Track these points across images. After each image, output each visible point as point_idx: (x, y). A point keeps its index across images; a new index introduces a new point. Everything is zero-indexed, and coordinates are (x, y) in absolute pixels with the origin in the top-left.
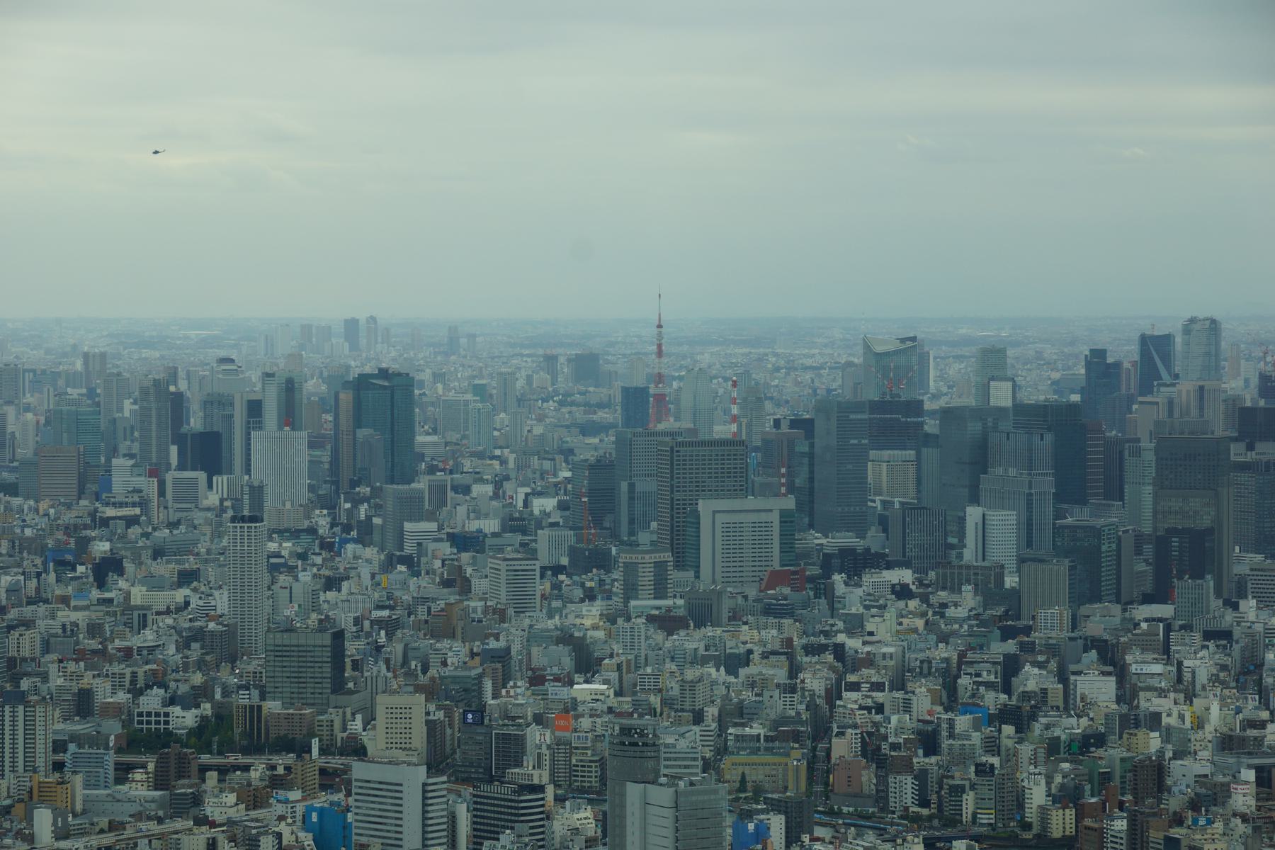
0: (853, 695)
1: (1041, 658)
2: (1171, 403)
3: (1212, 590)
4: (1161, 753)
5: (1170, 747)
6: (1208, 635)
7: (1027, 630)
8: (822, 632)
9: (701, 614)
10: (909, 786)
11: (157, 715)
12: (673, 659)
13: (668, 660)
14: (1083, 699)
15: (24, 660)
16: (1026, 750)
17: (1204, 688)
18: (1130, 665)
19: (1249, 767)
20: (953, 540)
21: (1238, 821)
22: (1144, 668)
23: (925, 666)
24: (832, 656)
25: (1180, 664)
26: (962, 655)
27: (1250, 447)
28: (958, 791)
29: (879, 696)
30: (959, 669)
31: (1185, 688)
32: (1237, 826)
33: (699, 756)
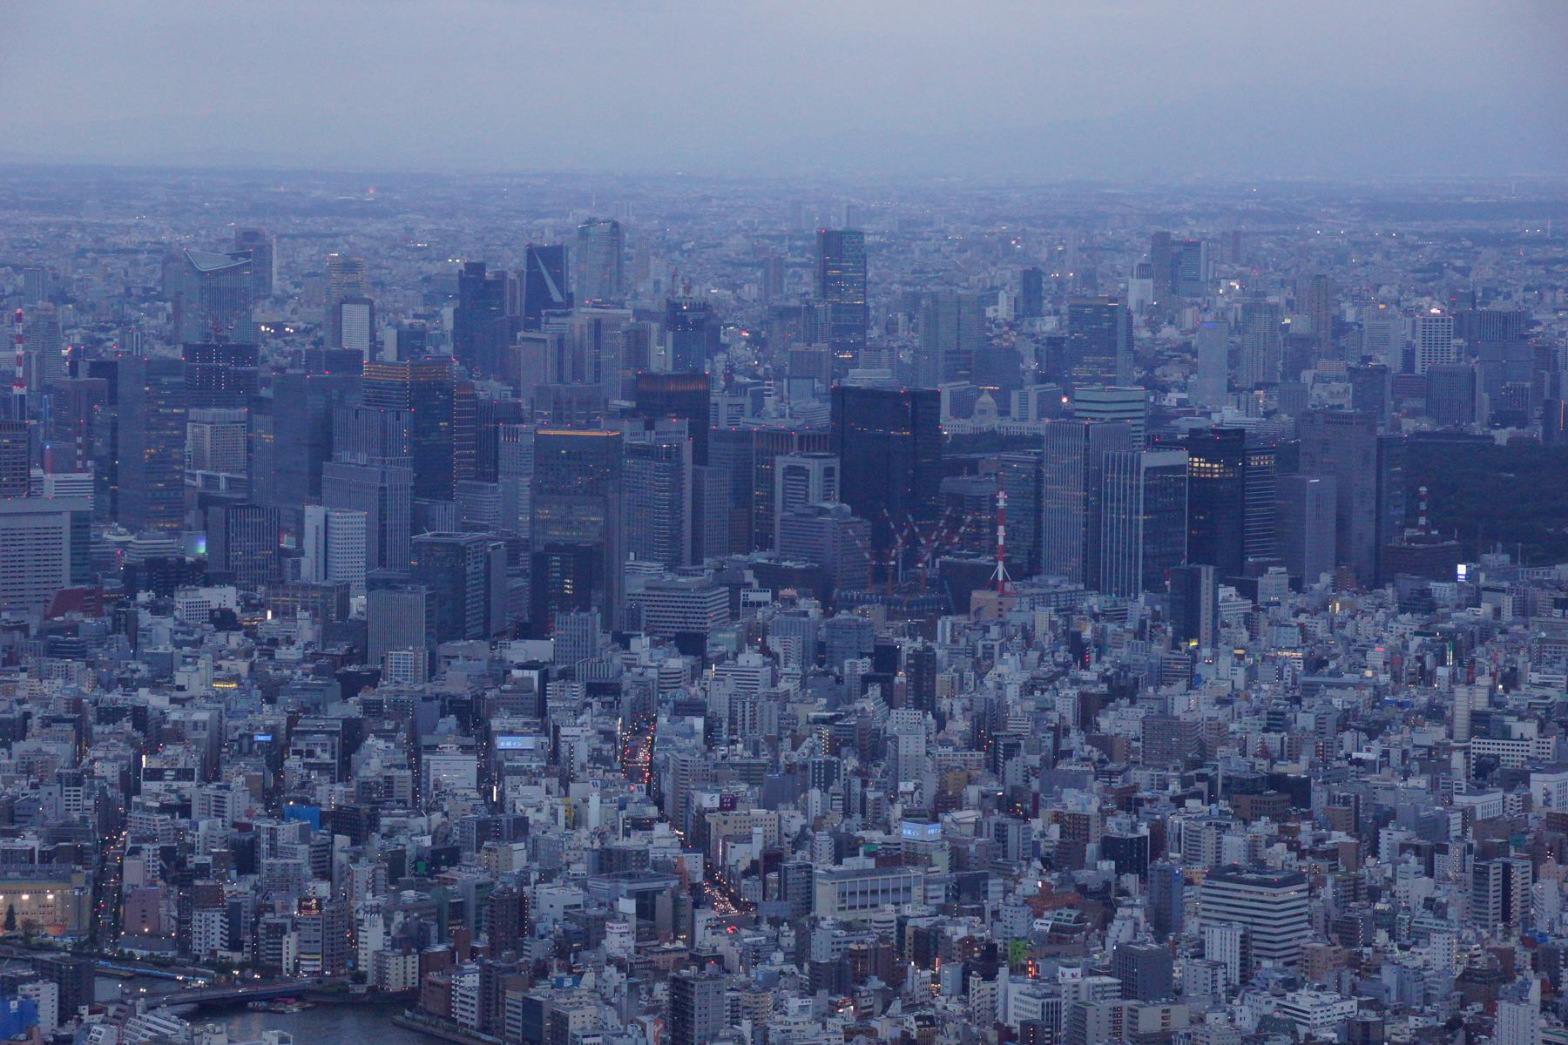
0: (155, 786)
2: (561, 341)
3: (598, 626)
4: (526, 872)
5: (536, 865)
6: (594, 689)
7: (373, 679)
8: (120, 680)
10: (218, 924)
14: (436, 786)
16: (363, 871)
17: (583, 767)
19: (630, 894)
20: (287, 542)
21: (612, 970)
26: (292, 720)
27: (649, 426)
29: (188, 787)
31: (557, 766)
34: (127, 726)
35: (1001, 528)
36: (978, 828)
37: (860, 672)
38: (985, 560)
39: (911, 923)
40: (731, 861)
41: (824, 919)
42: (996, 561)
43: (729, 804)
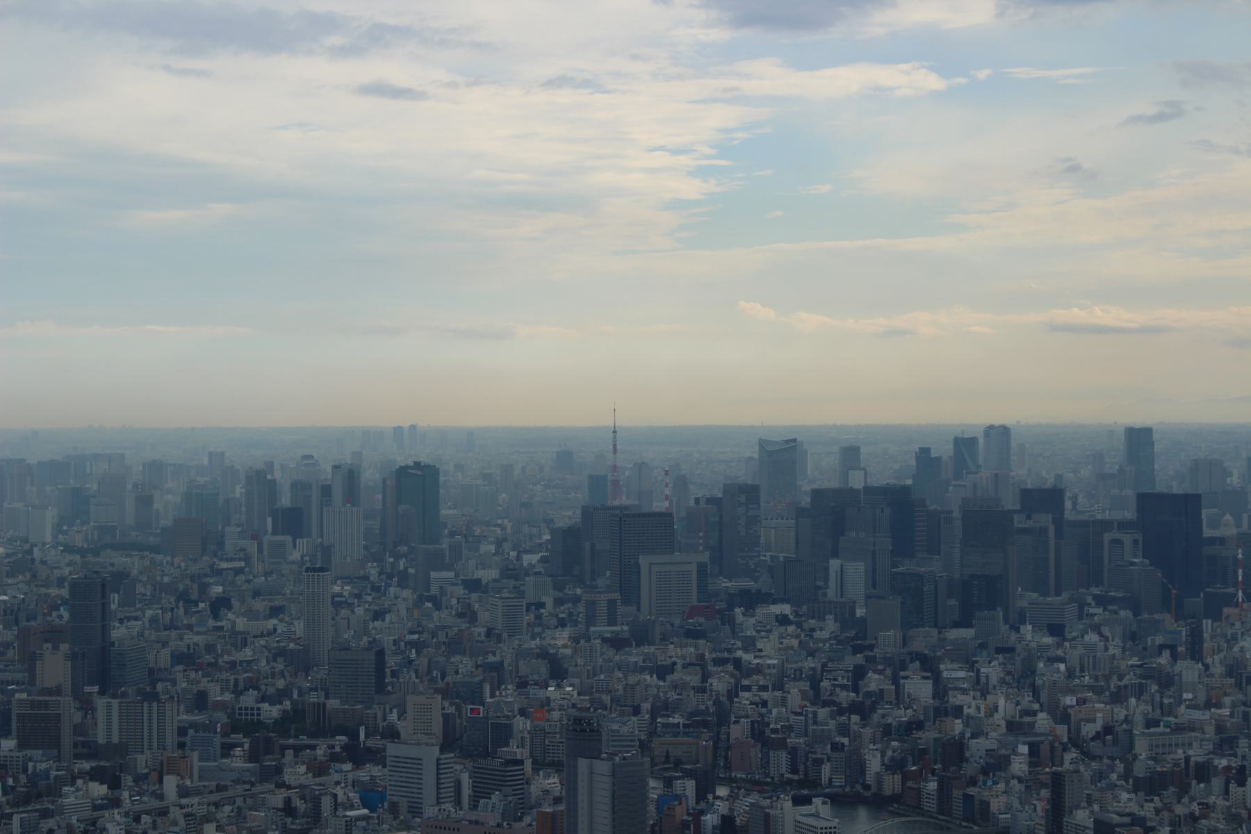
0: (747, 694)
1: (880, 667)
3: (1001, 620)
4: (962, 734)
5: (969, 730)
6: (999, 650)
7: (871, 647)
8: (726, 649)
9: (641, 636)
10: (784, 759)
11: (252, 709)
12: (620, 669)
13: (616, 670)
15: (160, 670)
16: (867, 732)
17: (994, 687)
18: (942, 671)
19: (1024, 743)
21: (1015, 782)
22: (953, 674)
23: (798, 673)
24: (732, 667)
25: (978, 670)
26: (824, 665)
27: (1029, 517)
28: (819, 762)
29: (765, 695)
30: (822, 676)
31: (981, 688)
32: (1015, 785)
33: (636, 738)
34: (731, 668)
35: (1240, 571)
36: (1232, 715)
37: (1157, 644)
38: (1231, 590)
39: (1193, 759)
40: (1084, 733)
41: (1141, 755)
42: (1238, 590)
43: (1082, 702)
